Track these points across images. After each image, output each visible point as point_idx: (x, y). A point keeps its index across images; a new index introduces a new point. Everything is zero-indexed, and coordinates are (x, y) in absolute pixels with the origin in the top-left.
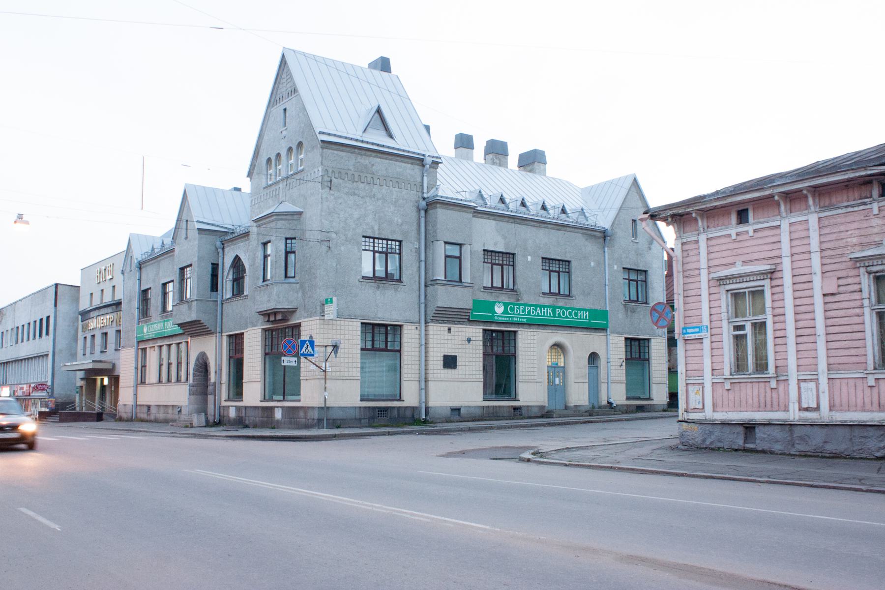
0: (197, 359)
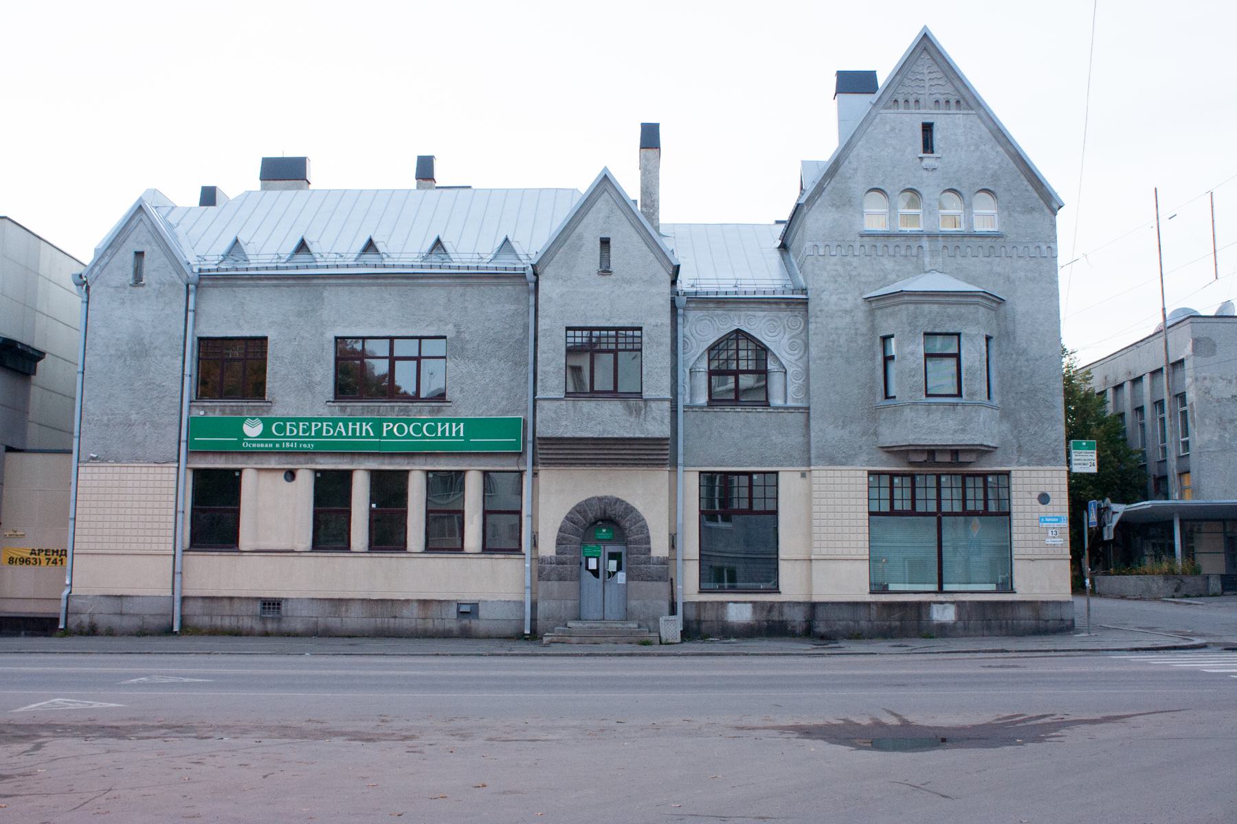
0: (580, 509)
